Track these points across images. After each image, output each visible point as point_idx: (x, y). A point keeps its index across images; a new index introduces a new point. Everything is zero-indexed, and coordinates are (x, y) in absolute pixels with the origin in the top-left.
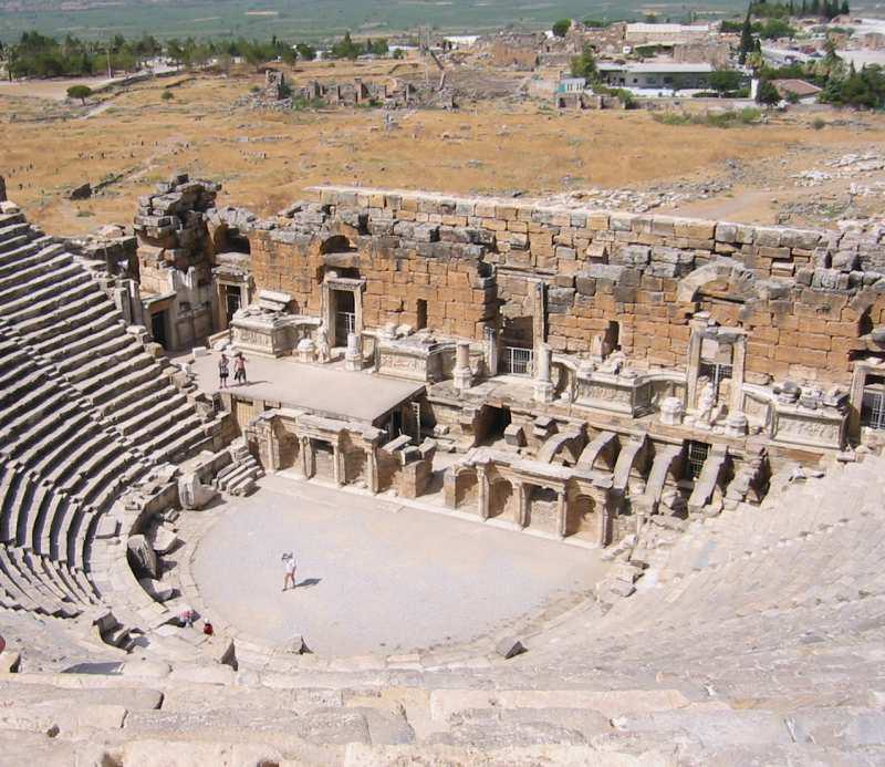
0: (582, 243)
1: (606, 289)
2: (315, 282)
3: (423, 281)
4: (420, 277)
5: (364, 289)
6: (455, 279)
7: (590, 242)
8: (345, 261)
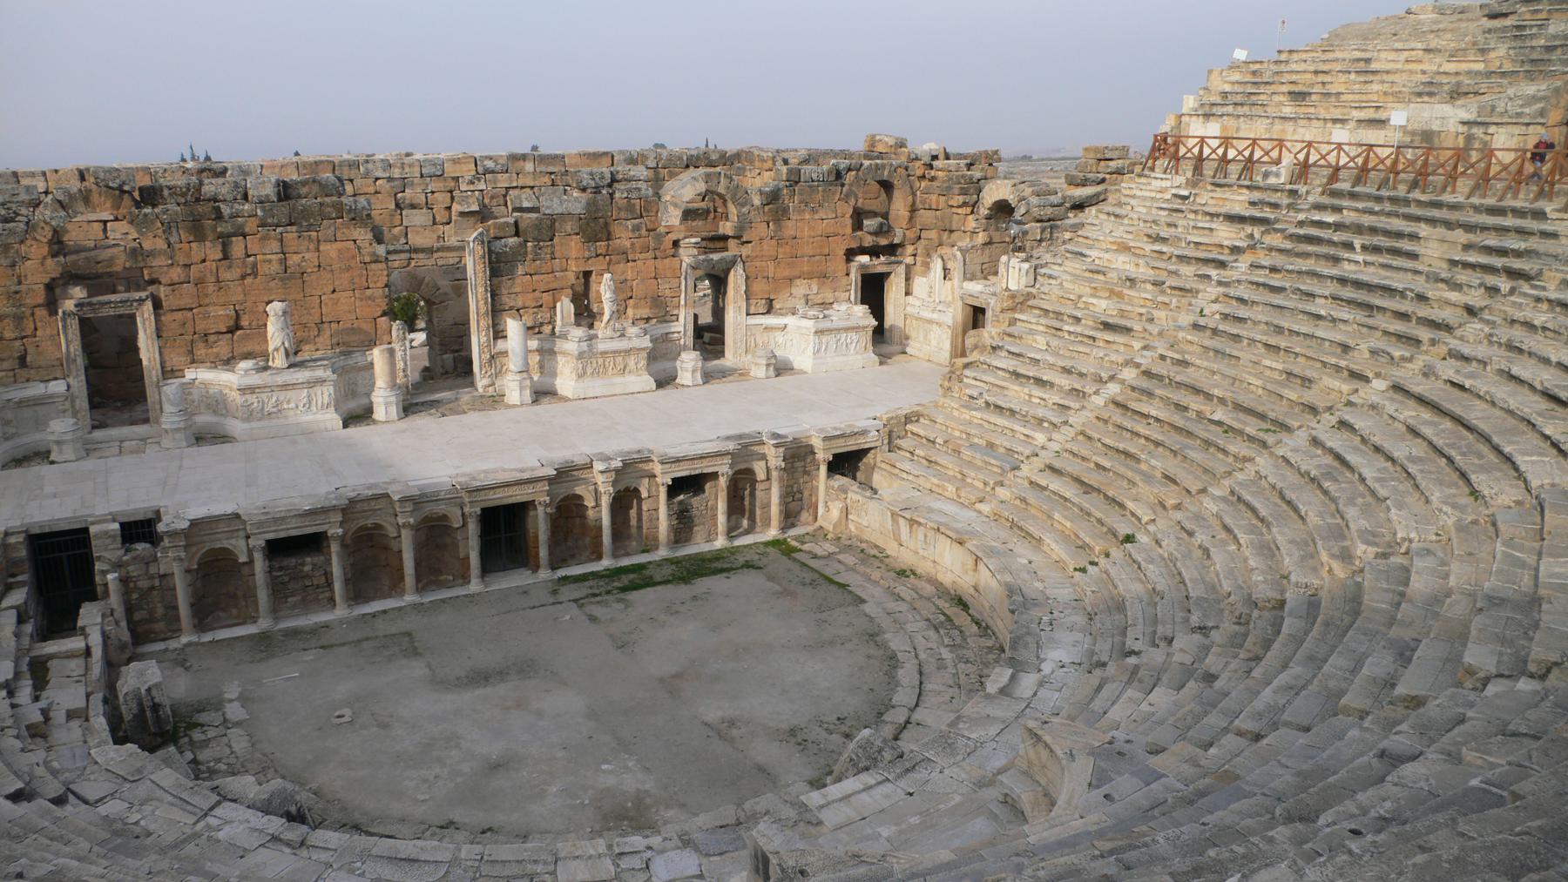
0: (442, 199)
1: (568, 228)
2: (42, 313)
3: (275, 267)
4: (270, 261)
5: (157, 305)
6: (333, 254)
7: (452, 198)
8: (112, 259)
